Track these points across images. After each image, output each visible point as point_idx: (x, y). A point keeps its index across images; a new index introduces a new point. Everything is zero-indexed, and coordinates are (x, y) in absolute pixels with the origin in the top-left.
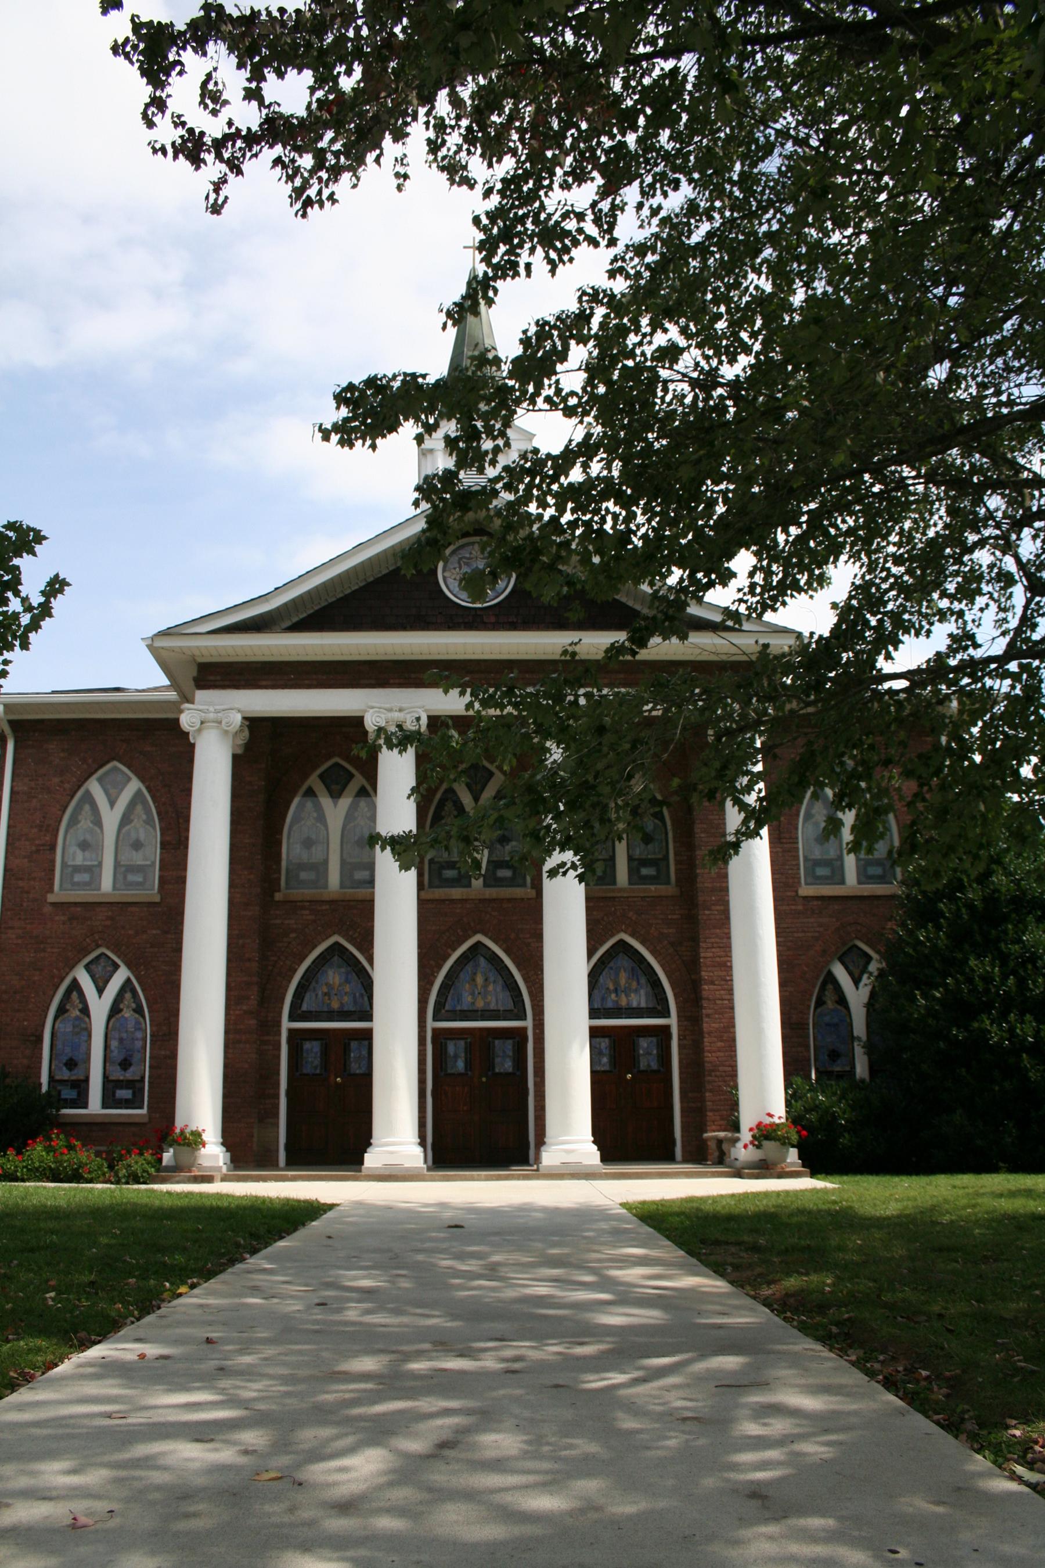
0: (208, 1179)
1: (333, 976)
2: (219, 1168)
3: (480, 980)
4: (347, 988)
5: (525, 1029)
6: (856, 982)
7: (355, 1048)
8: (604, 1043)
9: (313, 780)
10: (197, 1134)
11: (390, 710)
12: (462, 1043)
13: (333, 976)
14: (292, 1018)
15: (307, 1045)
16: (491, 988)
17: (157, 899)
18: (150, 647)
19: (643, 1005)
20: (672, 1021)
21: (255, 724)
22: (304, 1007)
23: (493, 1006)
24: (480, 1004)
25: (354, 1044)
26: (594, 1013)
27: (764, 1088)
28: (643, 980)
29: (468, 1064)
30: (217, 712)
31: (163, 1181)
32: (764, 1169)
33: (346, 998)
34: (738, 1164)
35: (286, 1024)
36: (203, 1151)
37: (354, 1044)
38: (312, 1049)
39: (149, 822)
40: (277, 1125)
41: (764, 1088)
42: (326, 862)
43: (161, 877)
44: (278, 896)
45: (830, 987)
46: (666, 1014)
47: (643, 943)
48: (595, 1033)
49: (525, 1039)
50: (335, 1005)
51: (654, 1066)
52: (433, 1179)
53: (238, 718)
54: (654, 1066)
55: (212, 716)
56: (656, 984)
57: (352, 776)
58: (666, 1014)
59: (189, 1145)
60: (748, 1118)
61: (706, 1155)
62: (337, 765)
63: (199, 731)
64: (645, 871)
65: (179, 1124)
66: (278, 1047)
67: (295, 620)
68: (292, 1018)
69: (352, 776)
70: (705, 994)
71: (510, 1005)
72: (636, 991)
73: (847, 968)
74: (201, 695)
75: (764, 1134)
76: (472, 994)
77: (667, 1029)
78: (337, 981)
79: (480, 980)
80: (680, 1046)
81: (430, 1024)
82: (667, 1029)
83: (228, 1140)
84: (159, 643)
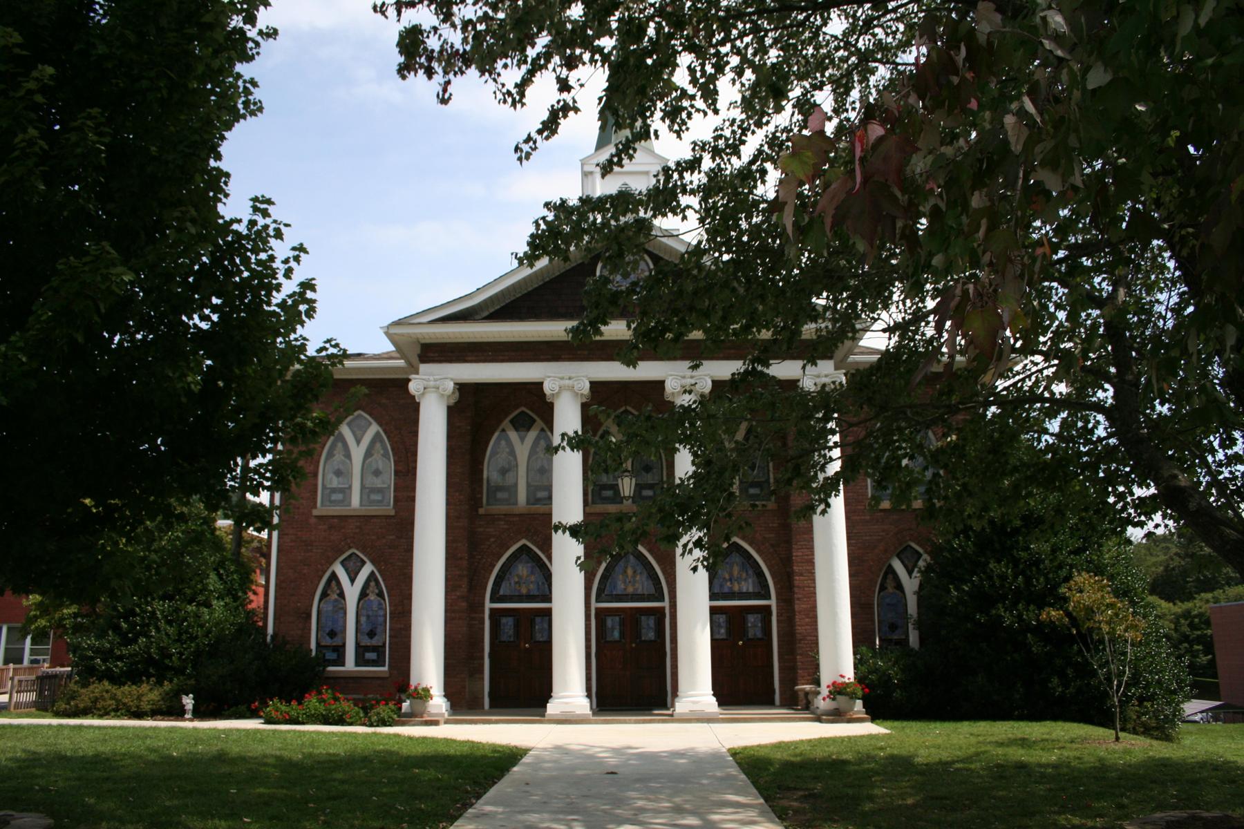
0: (435, 723)
1: (522, 569)
2: (443, 715)
3: (630, 572)
4: (533, 578)
5: (663, 608)
6: (910, 573)
7: (539, 623)
8: (722, 619)
9: (506, 423)
10: (427, 690)
11: (562, 379)
12: (617, 618)
13: (522, 569)
14: (492, 601)
15: (504, 620)
16: (638, 578)
17: (393, 513)
18: (386, 333)
19: (751, 590)
20: (773, 602)
21: (462, 388)
22: (501, 592)
23: (640, 591)
24: (630, 590)
25: (538, 620)
26: (713, 597)
27: (838, 656)
28: (750, 572)
29: (622, 634)
30: (435, 380)
31: (403, 724)
32: (837, 716)
33: (531, 586)
34: (819, 712)
35: (488, 605)
36: (431, 702)
37: (538, 620)
38: (508, 622)
39: (385, 455)
40: (483, 679)
41: (838, 656)
42: (516, 485)
43: (395, 497)
44: (481, 511)
45: (890, 576)
46: (768, 597)
47: (750, 545)
48: (714, 611)
50: (524, 591)
51: (759, 635)
52: (596, 722)
53: (451, 385)
54: (759, 635)
55: (432, 383)
56: (760, 574)
57: (534, 421)
58: (768, 597)
59: (421, 698)
60: (827, 677)
61: (797, 703)
62: (523, 412)
63: (423, 394)
64: (752, 491)
65: (413, 682)
66: (483, 623)
67: (492, 310)
68: (492, 601)
69: (534, 421)
70: (796, 583)
71: (653, 591)
72: (746, 580)
73: (903, 562)
74: (424, 368)
75: (838, 690)
76: (625, 582)
77: (767, 609)
78: (525, 573)
79: (630, 572)
80: (778, 621)
81: (594, 605)
82: (769, 607)
83: (448, 695)
84: (392, 331)
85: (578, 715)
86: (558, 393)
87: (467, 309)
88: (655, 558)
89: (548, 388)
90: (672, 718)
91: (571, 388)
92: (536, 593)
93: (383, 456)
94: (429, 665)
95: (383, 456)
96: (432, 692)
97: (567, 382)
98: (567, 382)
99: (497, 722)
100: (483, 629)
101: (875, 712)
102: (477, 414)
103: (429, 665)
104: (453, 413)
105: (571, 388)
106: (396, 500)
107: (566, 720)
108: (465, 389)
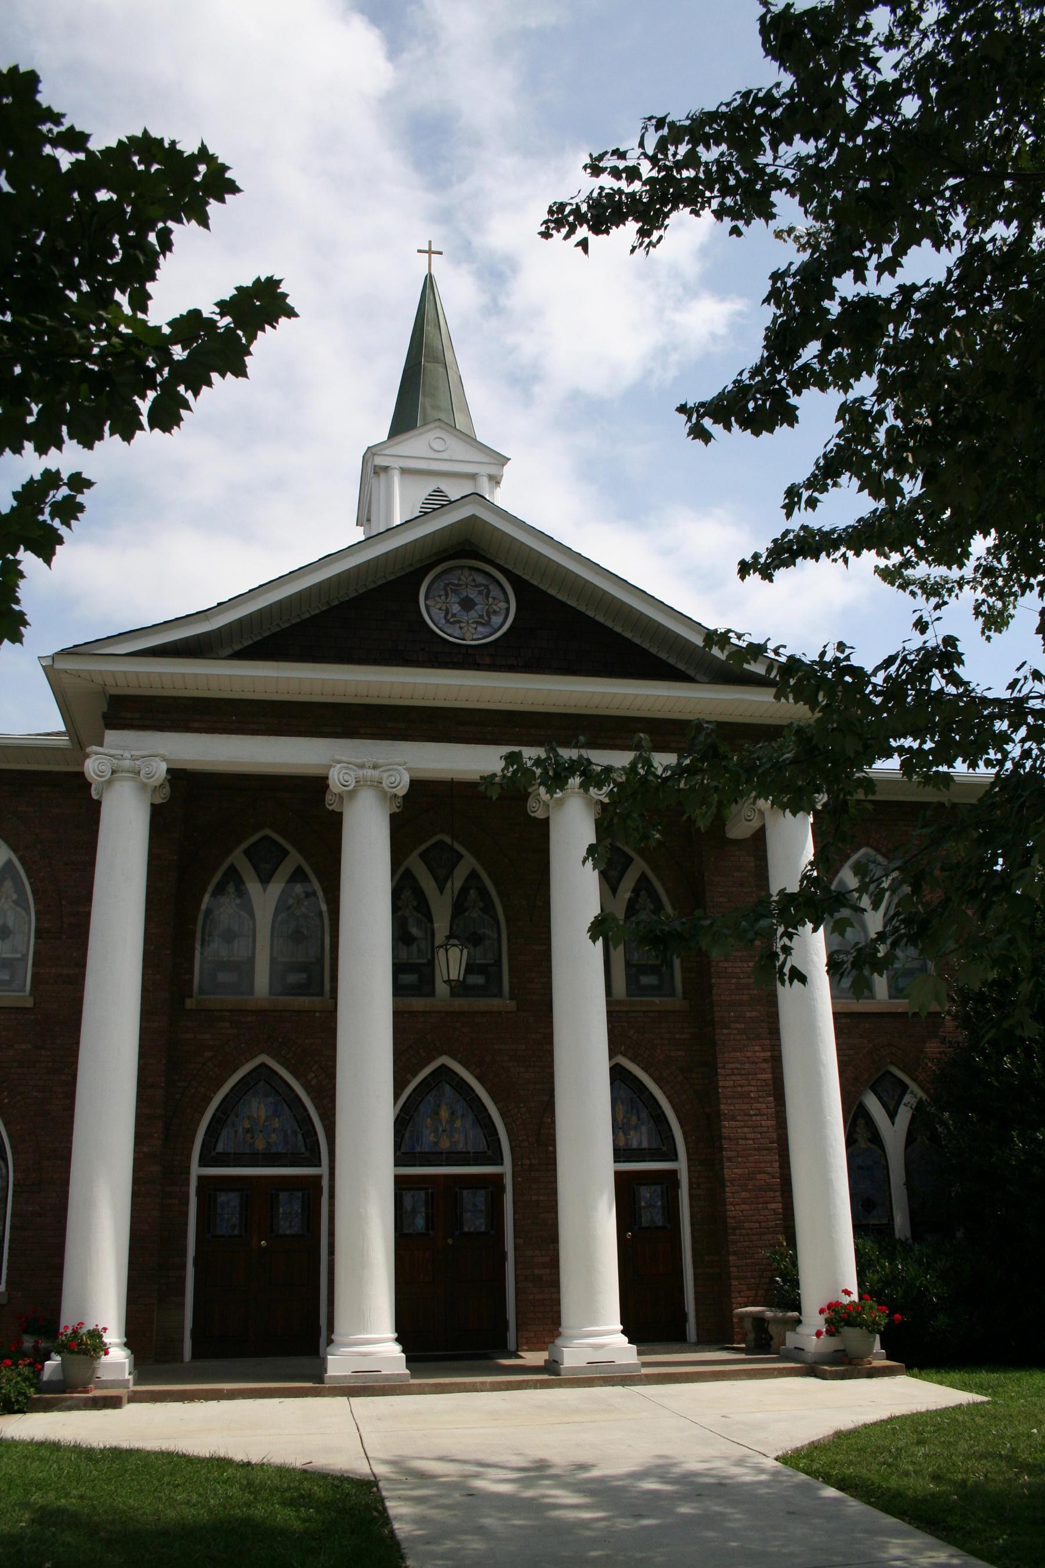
0: (113, 1403)
1: (258, 1108)
2: (123, 1384)
3: (444, 1114)
4: (276, 1123)
5: (500, 1177)
6: (892, 1115)
9: (238, 858)
10: (96, 1335)
11: (362, 766)
12: (422, 1194)
13: (258, 1108)
14: (203, 1163)
15: (222, 1198)
16: (458, 1123)
17: (29, 1003)
18: (50, 672)
19: (645, 1145)
20: (681, 1166)
21: (178, 776)
22: (220, 1148)
23: (461, 1147)
24: (445, 1144)
25: (283, 1196)
27: (831, 1259)
28: (644, 1115)
29: (429, 1220)
30: (133, 758)
31: (47, 1407)
32: (843, 1364)
33: (274, 1137)
34: (810, 1358)
35: (196, 1170)
36: (104, 1359)
37: (283, 1196)
38: (229, 1201)
39: (21, 902)
40: (182, 1305)
41: (831, 1259)
42: (251, 960)
43: (34, 975)
44: (190, 1003)
45: (861, 1121)
46: (673, 1157)
47: (645, 1069)
49: (502, 1189)
50: (260, 1146)
51: (659, 1221)
52: (421, 1390)
53: (164, 767)
54: (659, 1221)
55: (127, 763)
56: (659, 1118)
57: (286, 853)
58: (673, 1157)
59: (86, 1352)
60: (814, 1296)
61: (764, 1346)
62: (267, 838)
63: (109, 782)
64: (645, 980)
65: (68, 1320)
66: (186, 1202)
67: (238, 647)
68: (203, 1163)
69: (286, 853)
70: (725, 1132)
71: (483, 1146)
72: (636, 1128)
73: (880, 1099)
74: (111, 736)
75: (839, 1318)
76: (436, 1131)
77: (672, 1176)
78: (263, 1114)
79: (444, 1114)
80: (691, 1197)
83: (133, 1340)
84: (61, 665)
85: (387, 1377)
86: (352, 794)
87: (197, 637)
88: (489, 1091)
89: (337, 778)
90: (552, 1373)
91: (377, 785)
92: (281, 1149)
93: (17, 903)
94: (100, 1289)
95: (17, 903)
96: (106, 1339)
97: (369, 773)
98: (369, 773)
99: (232, 1395)
100: (186, 1215)
101: (913, 1354)
102: (197, 824)
103: (100, 1289)
104: (162, 822)
105: (377, 785)
106: (37, 980)
107: (367, 1386)
108: (183, 781)
